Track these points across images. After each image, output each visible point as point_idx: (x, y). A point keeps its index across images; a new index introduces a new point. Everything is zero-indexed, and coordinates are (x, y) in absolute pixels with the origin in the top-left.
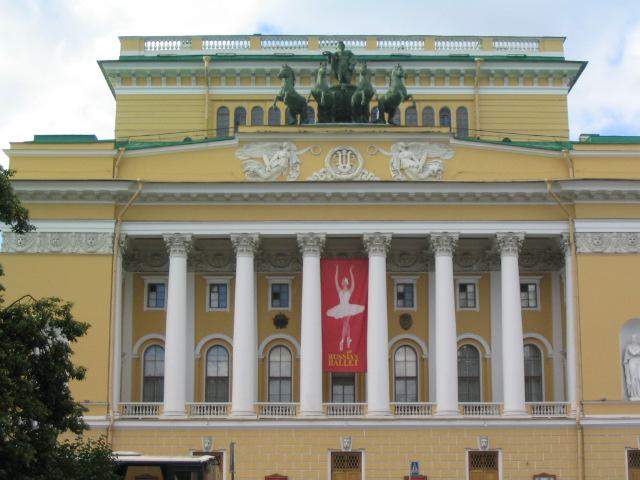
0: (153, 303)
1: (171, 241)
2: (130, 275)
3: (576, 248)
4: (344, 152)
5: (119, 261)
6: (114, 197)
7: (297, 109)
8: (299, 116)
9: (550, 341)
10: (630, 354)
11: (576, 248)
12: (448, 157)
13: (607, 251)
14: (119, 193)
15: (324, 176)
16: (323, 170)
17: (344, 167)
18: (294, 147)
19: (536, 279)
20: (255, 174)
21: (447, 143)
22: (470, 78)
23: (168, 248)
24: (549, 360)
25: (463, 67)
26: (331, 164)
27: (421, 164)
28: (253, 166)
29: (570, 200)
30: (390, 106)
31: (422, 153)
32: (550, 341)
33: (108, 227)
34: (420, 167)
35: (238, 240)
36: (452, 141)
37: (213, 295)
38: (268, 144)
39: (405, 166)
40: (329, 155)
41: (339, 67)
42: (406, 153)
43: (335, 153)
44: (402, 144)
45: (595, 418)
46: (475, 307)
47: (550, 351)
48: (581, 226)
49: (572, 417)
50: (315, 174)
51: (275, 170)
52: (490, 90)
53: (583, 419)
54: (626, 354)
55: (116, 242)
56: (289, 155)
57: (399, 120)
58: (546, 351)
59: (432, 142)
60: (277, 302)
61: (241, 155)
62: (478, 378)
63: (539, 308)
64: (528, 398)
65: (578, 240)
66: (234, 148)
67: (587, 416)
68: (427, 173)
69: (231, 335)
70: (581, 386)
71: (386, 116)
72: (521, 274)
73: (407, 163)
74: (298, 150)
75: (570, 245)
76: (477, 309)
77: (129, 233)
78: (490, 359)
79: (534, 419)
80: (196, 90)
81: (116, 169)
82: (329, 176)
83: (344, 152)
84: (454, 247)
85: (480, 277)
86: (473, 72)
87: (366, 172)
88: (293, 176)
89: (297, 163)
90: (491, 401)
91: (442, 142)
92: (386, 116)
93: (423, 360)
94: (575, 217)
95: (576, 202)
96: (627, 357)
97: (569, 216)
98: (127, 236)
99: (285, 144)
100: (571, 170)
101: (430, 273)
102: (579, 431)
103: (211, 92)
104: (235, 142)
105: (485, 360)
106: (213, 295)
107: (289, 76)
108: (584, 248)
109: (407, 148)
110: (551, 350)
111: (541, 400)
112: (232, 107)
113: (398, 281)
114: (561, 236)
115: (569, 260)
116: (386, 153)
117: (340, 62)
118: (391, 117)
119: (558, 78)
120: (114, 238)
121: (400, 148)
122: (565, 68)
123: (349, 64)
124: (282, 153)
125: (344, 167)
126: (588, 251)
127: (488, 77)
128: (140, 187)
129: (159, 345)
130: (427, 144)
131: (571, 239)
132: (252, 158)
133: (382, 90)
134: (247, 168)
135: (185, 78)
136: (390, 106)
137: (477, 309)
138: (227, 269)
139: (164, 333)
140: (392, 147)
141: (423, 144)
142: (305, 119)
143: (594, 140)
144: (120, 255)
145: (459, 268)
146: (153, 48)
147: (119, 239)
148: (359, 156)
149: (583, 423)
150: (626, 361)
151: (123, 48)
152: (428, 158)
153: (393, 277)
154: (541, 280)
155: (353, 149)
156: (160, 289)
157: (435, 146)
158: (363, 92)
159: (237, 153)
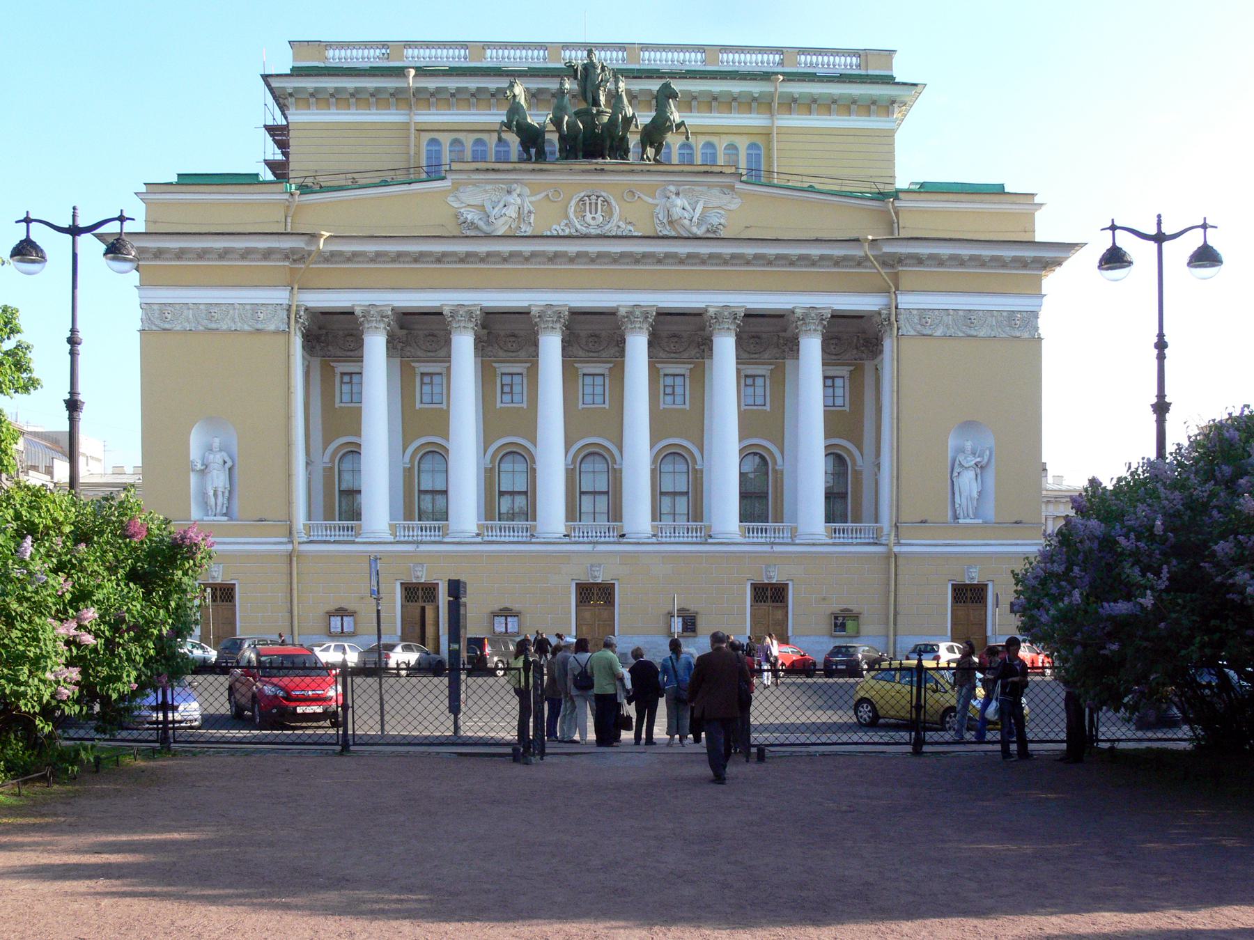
0: (346, 398)
1: (365, 315)
2: (316, 362)
4: (593, 197)
5: (297, 342)
6: (287, 257)
8: (533, 151)
9: (860, 448)
10: (961, 465)
11: (898, 329)
12: (732, 207)
14: (293, 251)
17: (594, 218)
18: (527, 191)
19: (844, 371)
20: (473, 225)
21: (732, 188)
23: (361, 324)
24: (857, 474)
26: (575, 211)
29: (892, 266)
31: (697, 202)
32: (860, 448)
33: (280, 296)
34: (695, 219)
35: (453, 314)
36: (738, 186)
37: (424, 387)
39: (675, 217)
40: (573, 203)
41: (589, 85)
42: (679, 202)
43: (580, 200)
44: (672, 188)
45: (914, 546)
47: (859, 461)
49: (884, 542)
50: (554, 227)
54: (956, 465)
55: (293, 316)
57: (669, 154)
59: (710, 186)
60: (507, 398)
62: (767, 493)
63: (847, 409)
64: (829, 518)
65: (901, 317)
68: (703, 229)
73: (677, 212)
74: (533, 194)
75: (890, 324)
76: (768, 408)
77: (310, 305)
79: (834, 544)
81: (289, 220)
82: (573, 231)
83: (593, 197)
84: (738, 326)
85: (772, 367)
89: (530, 212)
90: (782, 522)
91: (727, 187)
93: (695, 470)
94: (897, 289)
98: (306, 309)
101: (706, 361)
105: (775, 471)
106: (424, 387)
108: (907, 329)
109: (677, 194)
110: (861, 461)
113: (667, 371)
115: (888, 344)
116: (650, 200)
118: (658, 152)
120: (289, 310)
125: (594, 218)
126: (912, 333)
127: (791, 104)
129: (354, 451)
130: (704, 189)
131: (893, 318)
134: (462, 219)
138: (442, 353)
139: (358, 433)
141: (697, 188)
142: (541, 156)
143: (926, 189)
144: (299, 334)
145: (745, 355)
147: (297, 312)
148: (614, 203)
153: (659, 366)
155: (603, 194)
156: (355, 378)
157: (716, 191)
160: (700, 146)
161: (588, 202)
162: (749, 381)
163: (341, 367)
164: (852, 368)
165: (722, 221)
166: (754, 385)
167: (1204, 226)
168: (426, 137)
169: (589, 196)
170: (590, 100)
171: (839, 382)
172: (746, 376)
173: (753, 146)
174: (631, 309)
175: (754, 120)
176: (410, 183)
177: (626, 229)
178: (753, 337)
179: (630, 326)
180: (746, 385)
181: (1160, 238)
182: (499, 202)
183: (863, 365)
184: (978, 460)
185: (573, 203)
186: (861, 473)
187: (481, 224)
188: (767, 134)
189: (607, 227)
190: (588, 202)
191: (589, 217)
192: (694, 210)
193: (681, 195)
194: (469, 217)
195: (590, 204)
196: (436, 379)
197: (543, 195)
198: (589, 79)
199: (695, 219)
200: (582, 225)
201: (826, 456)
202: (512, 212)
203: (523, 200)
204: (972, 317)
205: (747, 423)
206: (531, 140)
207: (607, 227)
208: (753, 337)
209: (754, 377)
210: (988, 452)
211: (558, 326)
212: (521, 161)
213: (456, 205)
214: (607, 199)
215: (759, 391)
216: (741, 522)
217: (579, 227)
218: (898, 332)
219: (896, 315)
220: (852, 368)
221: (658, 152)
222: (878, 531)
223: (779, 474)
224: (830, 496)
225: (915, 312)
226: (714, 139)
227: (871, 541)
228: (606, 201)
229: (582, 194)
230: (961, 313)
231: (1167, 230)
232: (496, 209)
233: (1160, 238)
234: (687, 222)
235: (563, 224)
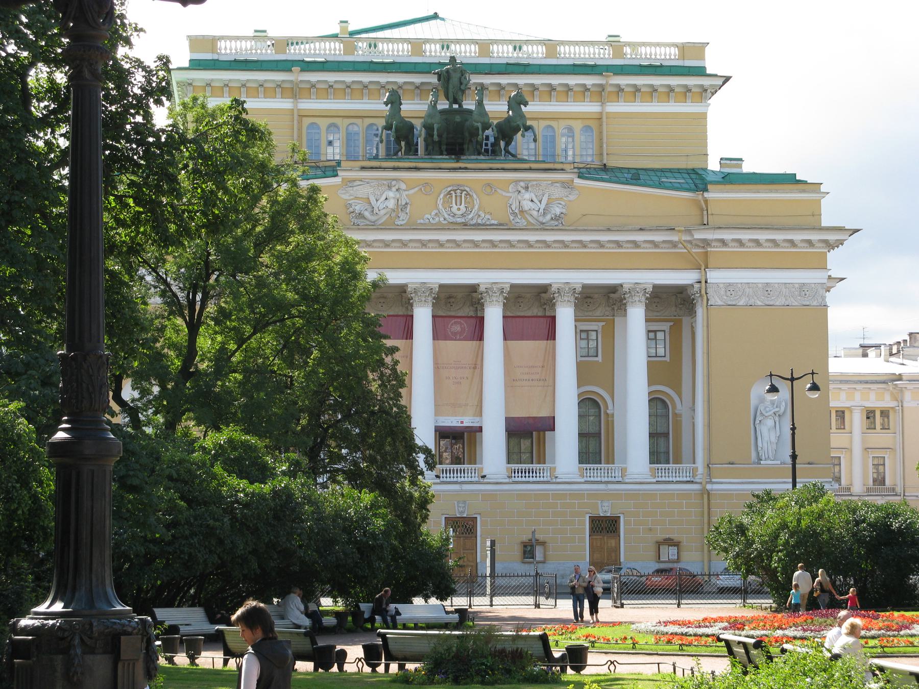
3: (708, 300)
8: (403, 143)
9: (680, 395)
10: (761, 413)
11: (708, 300)
13: (741, 303)
15: (437, 219)
16: (436, 211)
17: (459, 209)
18: (403, 186)
19: (666, 326)
20: (361, 216)
25: (589, 81)
27: (543, 206)
32: (680, 395)
34: (541, 211)
39: (526, 208)
40: (442, 196)
41: (451, 86)
42: (527, 196)
43: (449, 193)
44: (522, 184)
46: (597, 356)
47: (679, 406)
48: (714, 276)
51: (383, 212)
53: (711, 482)
56: (398, 196)
58: (674, 407)
63: (667, 359)
67: (714, 480)
68: (548, 217)
70: (709, 449)
71: (502, 144)
72: (647, 321)
73: (527, 205)
75: (701, 296)
76: (599, 359)
78: (613, 415)
79: (658, 482)
86: (602, 87)
87: (483, 215)
88: (403, 219)
89: (406, 204)
92: (502, 144)
95: (709, 249)
96: (759, 418)
97: (703, 264)
99: (394, 183)
100: (705, 212)
102: (705, 496)
107: (395, 101)
108: (715, 300)
109: (527, 188)
110: (680, 407)
111: (669, 463)
114: (692, 285)
115: (700, 312)
121: (520, 189)
122: (705, 82)
123: (461, 84)
124: (391, 194)
125: (459, 209)
126: (720, 303)
131: (703, 292)
132: (356, 198)
133: (497, 109)
134: (351, 210)
137: (599, 359)
146: (227, 50)
148: (475, 196)
149: (709, 487)
150: (757, 422)
151: (193, 49)
154: (671, 326)
158: (479, 125)
160: (541, 129)
161: (454, 195)
164: (672, 324)
165: (564, 211)
166: (588, 339)
167: (813, 373)
168: (307, 122)
169: (455, 191)
170: (451, 99)
171: (660, 336)
172: (581, 331)
173: (587, 128)
174: (490, 286)
175: (591, 108)
176: (308, 180)
177: (484, 218)
178: (587, 297)
179: (488, 299)
180: (581, 339)
181: (792, 379)
182: (381, 195)
183: (681, 321)
184: (777, 410)
185: (442, 196)
186: (680, 415)
187: (367, 214)
188: (599, 118)
189: (470, 216)
190: (454, 195)
191: (455, 208)
192: (540, 202)
193: (530, 189)
194: (357, 208)
195: (456, 196)
197: (416, 189)
198: (451, 81)
199: (541, 211)
200: (449, 215)
201: (650, 401)
202: (391, 204)
203: (401, 195)
204: (769, 290)
205: (584, 373)
207: (470, 216)
208: (587, 297)
209: (587, 331)
210: (784, 404)
211: (430, 299)
213: (346, 197)
214: (471, 193)
215: (592, 344)
216: (581, 462)
217: (446, 216)
218: (707, 303)
219: (706, 289)
220: (672, 324)
221: (508, 144)
222: (695, 470)
223: (610, 418)
224: (653, 436)
225: (721, 286)
226: (553, 124)
227: (688, 479)
228: (469, 194)
229: (449, 189)
230: (760, 286)
231: (795, 376)
232: (379, 202)
233: (792, 379)
234: (535, 213)
235: (433, 213)
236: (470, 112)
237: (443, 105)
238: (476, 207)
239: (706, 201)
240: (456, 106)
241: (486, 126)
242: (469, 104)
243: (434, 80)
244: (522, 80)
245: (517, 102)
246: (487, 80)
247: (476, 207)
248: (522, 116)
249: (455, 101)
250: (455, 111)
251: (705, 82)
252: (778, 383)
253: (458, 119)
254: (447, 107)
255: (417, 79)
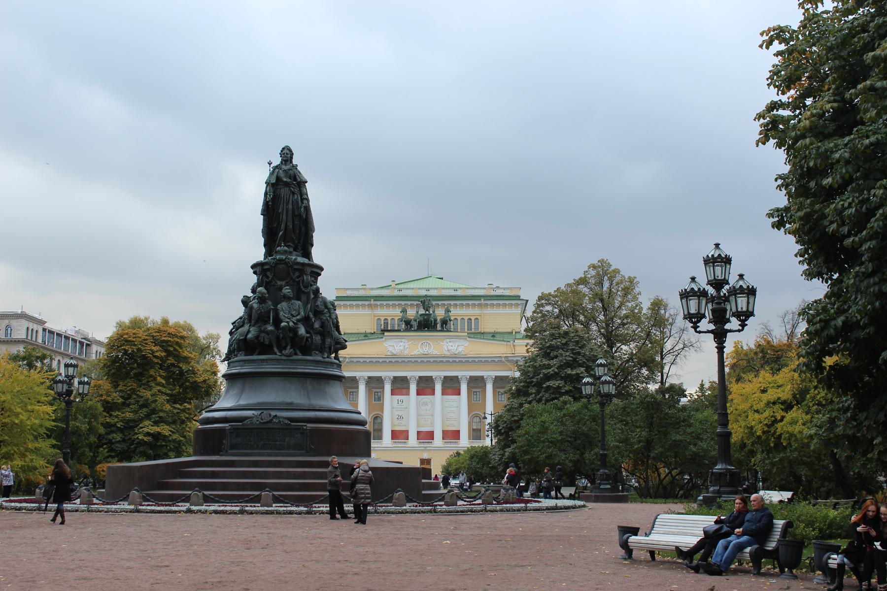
7: (408, 325)
18: (406, 341)
21: (466, 339)
22: (480, 305)
27: (455, 348)
28: (391, 349)
30: (445, 322)
36: (468, 339)
38: (396, 340)
42: (450, 344)
44: (448, 340)
52: (489, 311)
59: (460, 339)
61: (385, 344)
66: (383, 341)
69: (383, 412)
73: (450, 348)
80: (367, 311)
103: (375, 312)
104: (384, 339)
107: (404, 311)
112: (382, 319)
117: (425, 302)
119: (517, 305)
124: (402, 344)
128: (347, 360)
135: (363, 306)
136: (445, 322)
140: (444, 341)
146: (349, 293)
148: (432, 346)
152: (458, 346)
156: (354, 393)
157: (461, 341)
159: (384, 344)
162: (475, 393)
163: (350, 390)
196: (379, 394)
206: (408, 323)
212: (406, 330)
233: (491, 415)
236: (431, 314)
237: (422, 311)
238: (432, 348)
239: (514, 346)
240: (427, 312)
241: (435, 320)
242: (431, 312)
243: (420, 303)
244: (452, 303)
245: (448, 311)
246: (440, 303)
247: (432, 348)
248: (449, 316)
249: (427, 310)
250: (427, 315)
251: (519, 302)
252: (487, 416)
253: (426, 318)
254: (424, 312)
255: (415, 303)
